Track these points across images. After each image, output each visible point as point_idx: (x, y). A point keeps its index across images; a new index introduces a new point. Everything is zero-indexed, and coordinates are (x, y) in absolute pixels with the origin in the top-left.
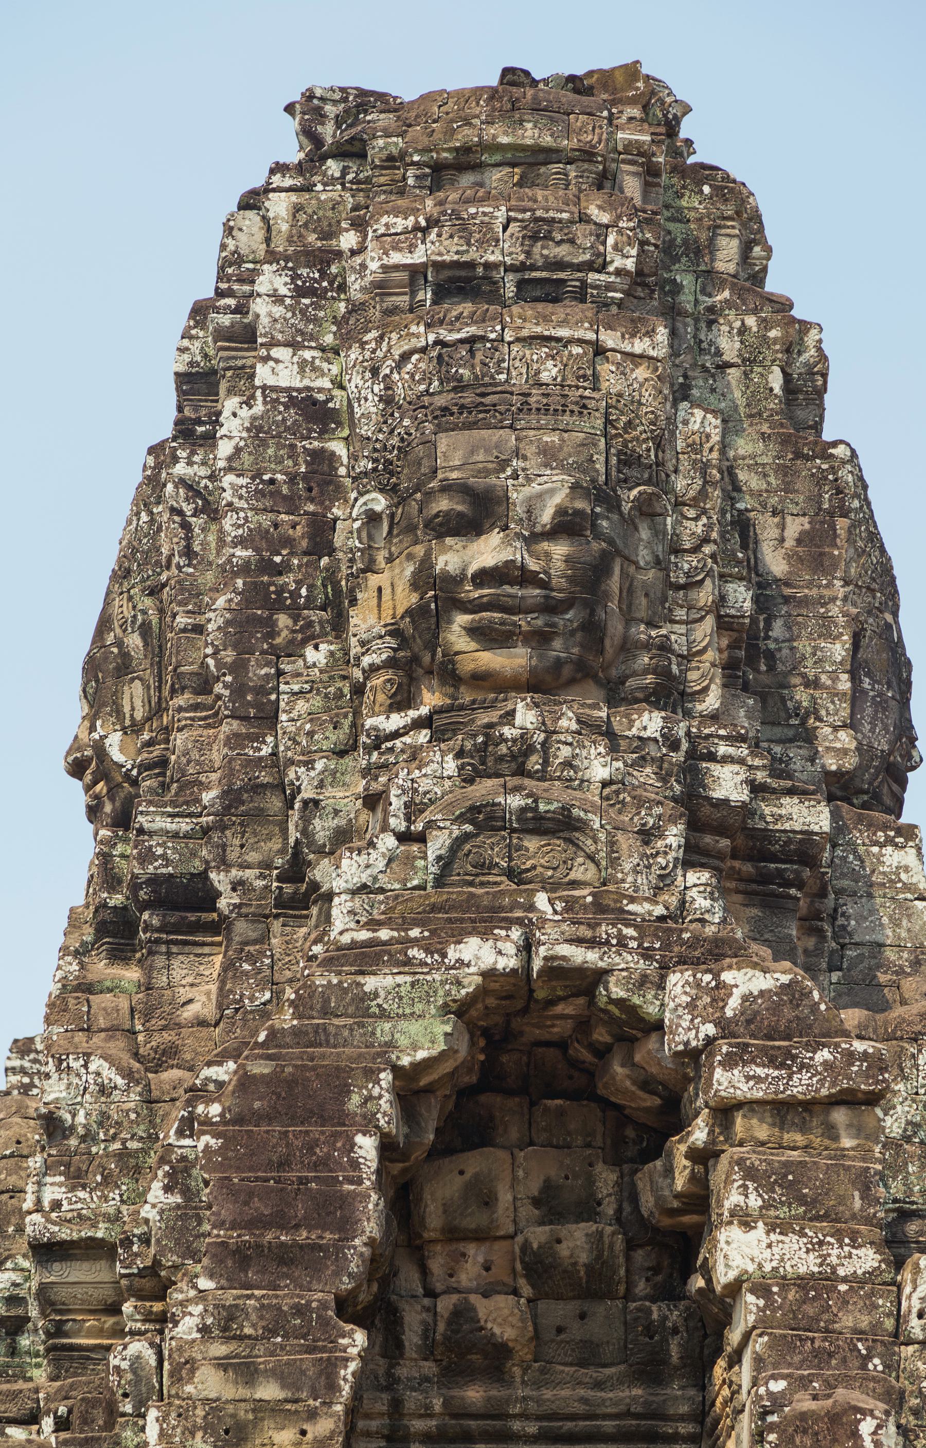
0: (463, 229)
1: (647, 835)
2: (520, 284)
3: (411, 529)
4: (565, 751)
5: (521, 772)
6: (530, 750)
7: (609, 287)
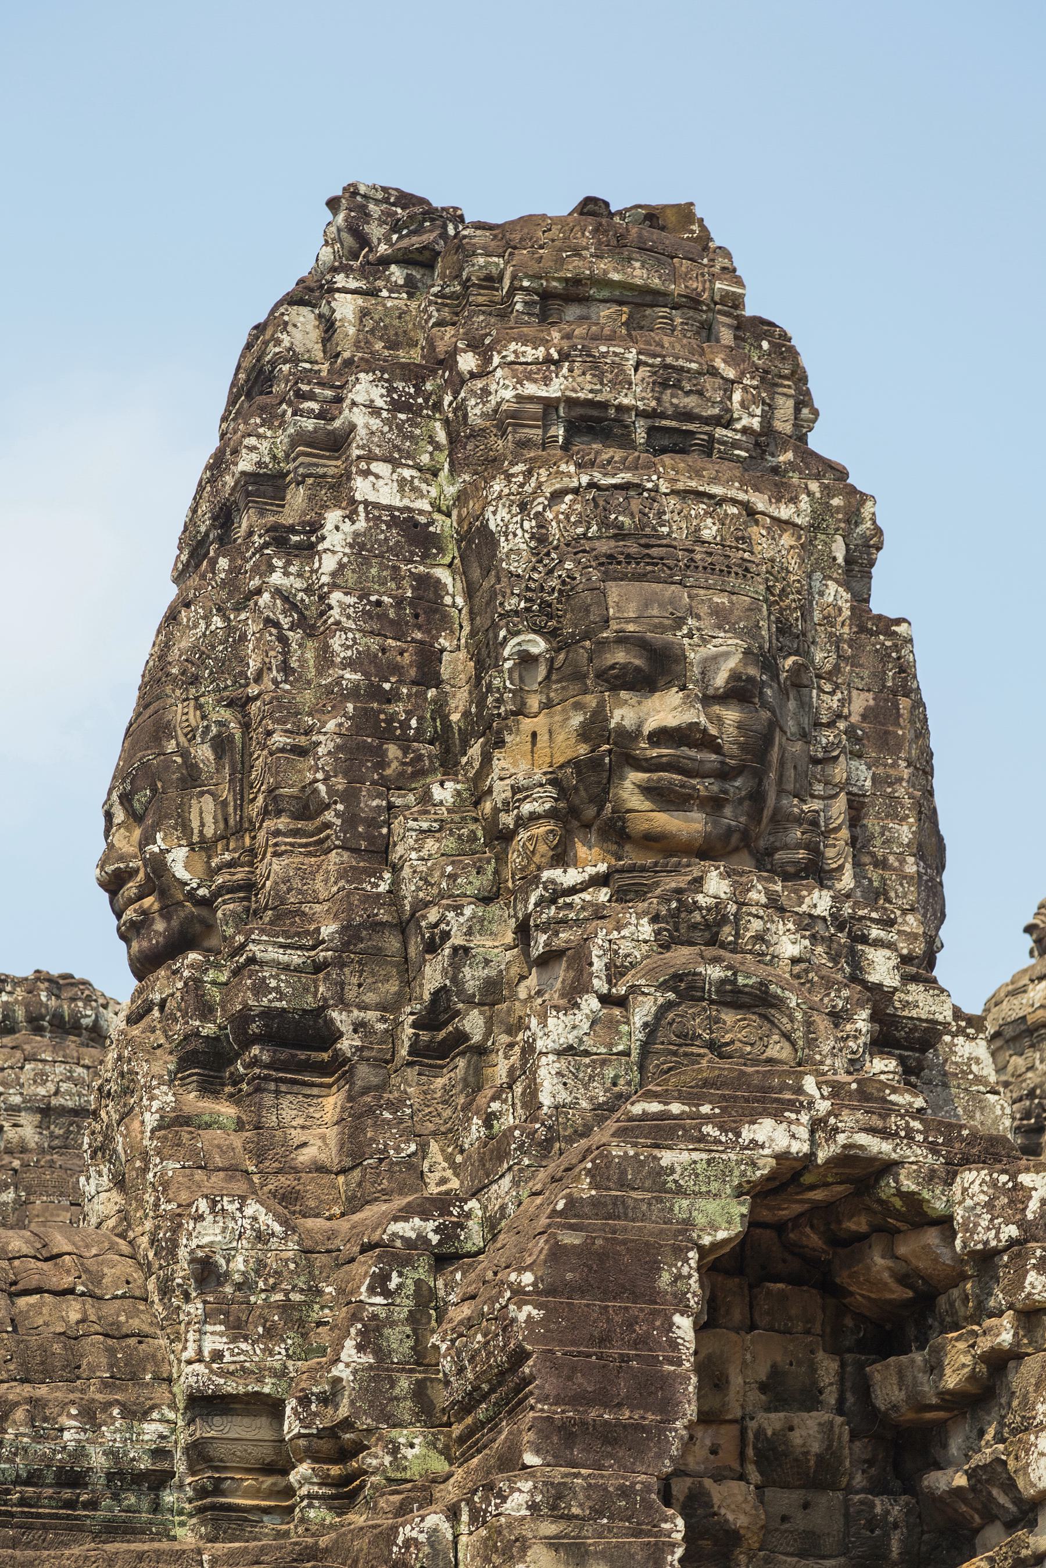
0: (594, 366)
1: (837, 1017)
2: (651, 431)
3: (578, 676)
4: (756, 925)
5: (713, 941)
6: (724, 920)
7: (736, 444)
